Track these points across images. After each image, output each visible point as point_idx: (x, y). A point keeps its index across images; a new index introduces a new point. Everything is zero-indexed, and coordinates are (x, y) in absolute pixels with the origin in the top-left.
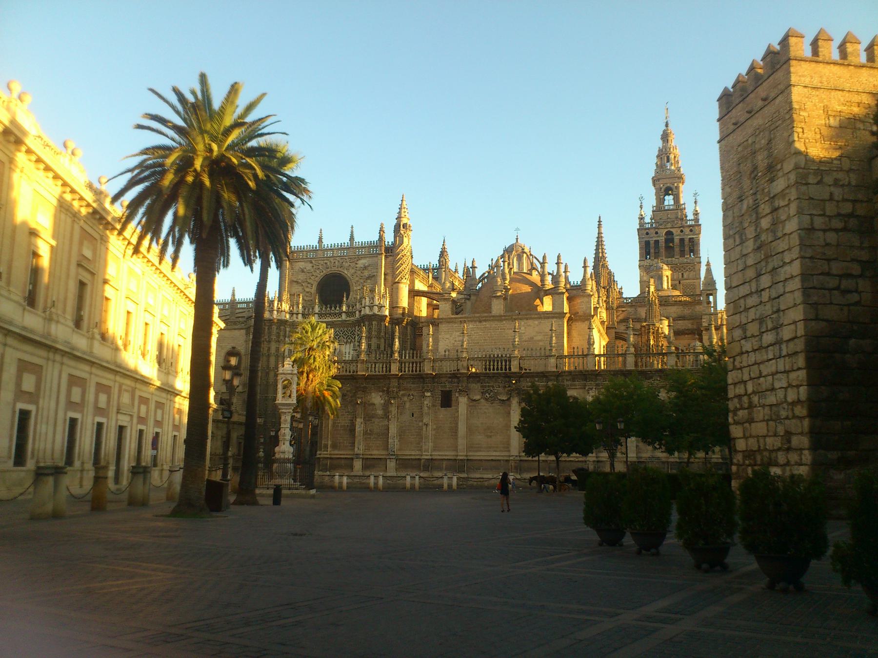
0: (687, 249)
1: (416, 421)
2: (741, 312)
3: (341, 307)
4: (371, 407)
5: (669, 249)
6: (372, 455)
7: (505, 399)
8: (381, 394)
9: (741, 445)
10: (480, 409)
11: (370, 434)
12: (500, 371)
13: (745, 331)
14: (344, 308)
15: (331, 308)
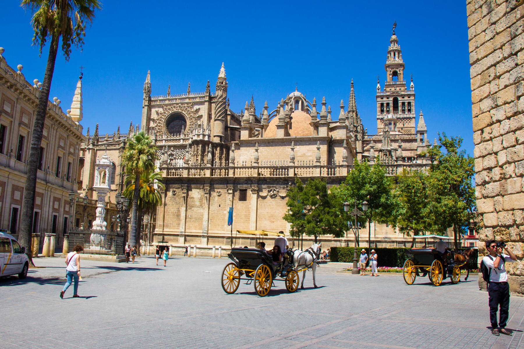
0: (406, 108)
1: (222, 210)
2: (490, 82)
3: (180, 135)
4: (192, 200)
5: (396, 108)
6: (191, 233)
7: (284, 195)
8: (198, 190)
9: (490, 220)
10: (266, 202)
11: (190, 219)
12: (281, 176)
13: (495, 100)
14: (182, 136)
15: (174, 135)
